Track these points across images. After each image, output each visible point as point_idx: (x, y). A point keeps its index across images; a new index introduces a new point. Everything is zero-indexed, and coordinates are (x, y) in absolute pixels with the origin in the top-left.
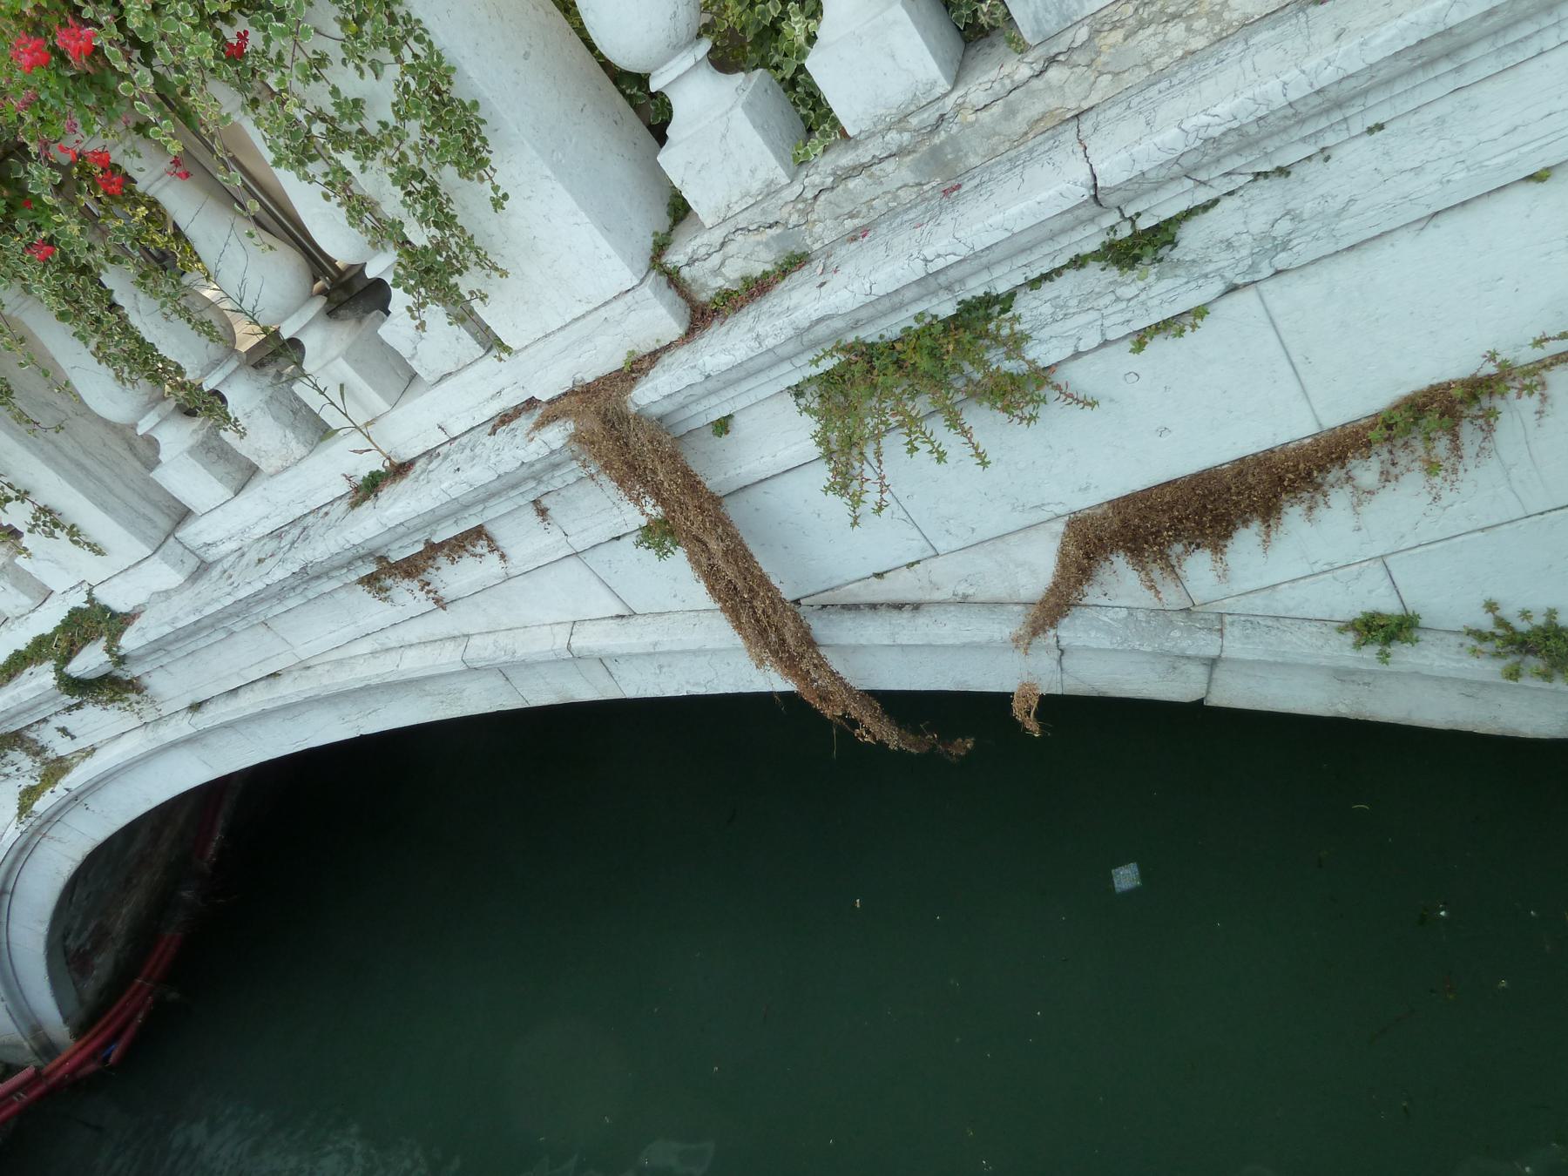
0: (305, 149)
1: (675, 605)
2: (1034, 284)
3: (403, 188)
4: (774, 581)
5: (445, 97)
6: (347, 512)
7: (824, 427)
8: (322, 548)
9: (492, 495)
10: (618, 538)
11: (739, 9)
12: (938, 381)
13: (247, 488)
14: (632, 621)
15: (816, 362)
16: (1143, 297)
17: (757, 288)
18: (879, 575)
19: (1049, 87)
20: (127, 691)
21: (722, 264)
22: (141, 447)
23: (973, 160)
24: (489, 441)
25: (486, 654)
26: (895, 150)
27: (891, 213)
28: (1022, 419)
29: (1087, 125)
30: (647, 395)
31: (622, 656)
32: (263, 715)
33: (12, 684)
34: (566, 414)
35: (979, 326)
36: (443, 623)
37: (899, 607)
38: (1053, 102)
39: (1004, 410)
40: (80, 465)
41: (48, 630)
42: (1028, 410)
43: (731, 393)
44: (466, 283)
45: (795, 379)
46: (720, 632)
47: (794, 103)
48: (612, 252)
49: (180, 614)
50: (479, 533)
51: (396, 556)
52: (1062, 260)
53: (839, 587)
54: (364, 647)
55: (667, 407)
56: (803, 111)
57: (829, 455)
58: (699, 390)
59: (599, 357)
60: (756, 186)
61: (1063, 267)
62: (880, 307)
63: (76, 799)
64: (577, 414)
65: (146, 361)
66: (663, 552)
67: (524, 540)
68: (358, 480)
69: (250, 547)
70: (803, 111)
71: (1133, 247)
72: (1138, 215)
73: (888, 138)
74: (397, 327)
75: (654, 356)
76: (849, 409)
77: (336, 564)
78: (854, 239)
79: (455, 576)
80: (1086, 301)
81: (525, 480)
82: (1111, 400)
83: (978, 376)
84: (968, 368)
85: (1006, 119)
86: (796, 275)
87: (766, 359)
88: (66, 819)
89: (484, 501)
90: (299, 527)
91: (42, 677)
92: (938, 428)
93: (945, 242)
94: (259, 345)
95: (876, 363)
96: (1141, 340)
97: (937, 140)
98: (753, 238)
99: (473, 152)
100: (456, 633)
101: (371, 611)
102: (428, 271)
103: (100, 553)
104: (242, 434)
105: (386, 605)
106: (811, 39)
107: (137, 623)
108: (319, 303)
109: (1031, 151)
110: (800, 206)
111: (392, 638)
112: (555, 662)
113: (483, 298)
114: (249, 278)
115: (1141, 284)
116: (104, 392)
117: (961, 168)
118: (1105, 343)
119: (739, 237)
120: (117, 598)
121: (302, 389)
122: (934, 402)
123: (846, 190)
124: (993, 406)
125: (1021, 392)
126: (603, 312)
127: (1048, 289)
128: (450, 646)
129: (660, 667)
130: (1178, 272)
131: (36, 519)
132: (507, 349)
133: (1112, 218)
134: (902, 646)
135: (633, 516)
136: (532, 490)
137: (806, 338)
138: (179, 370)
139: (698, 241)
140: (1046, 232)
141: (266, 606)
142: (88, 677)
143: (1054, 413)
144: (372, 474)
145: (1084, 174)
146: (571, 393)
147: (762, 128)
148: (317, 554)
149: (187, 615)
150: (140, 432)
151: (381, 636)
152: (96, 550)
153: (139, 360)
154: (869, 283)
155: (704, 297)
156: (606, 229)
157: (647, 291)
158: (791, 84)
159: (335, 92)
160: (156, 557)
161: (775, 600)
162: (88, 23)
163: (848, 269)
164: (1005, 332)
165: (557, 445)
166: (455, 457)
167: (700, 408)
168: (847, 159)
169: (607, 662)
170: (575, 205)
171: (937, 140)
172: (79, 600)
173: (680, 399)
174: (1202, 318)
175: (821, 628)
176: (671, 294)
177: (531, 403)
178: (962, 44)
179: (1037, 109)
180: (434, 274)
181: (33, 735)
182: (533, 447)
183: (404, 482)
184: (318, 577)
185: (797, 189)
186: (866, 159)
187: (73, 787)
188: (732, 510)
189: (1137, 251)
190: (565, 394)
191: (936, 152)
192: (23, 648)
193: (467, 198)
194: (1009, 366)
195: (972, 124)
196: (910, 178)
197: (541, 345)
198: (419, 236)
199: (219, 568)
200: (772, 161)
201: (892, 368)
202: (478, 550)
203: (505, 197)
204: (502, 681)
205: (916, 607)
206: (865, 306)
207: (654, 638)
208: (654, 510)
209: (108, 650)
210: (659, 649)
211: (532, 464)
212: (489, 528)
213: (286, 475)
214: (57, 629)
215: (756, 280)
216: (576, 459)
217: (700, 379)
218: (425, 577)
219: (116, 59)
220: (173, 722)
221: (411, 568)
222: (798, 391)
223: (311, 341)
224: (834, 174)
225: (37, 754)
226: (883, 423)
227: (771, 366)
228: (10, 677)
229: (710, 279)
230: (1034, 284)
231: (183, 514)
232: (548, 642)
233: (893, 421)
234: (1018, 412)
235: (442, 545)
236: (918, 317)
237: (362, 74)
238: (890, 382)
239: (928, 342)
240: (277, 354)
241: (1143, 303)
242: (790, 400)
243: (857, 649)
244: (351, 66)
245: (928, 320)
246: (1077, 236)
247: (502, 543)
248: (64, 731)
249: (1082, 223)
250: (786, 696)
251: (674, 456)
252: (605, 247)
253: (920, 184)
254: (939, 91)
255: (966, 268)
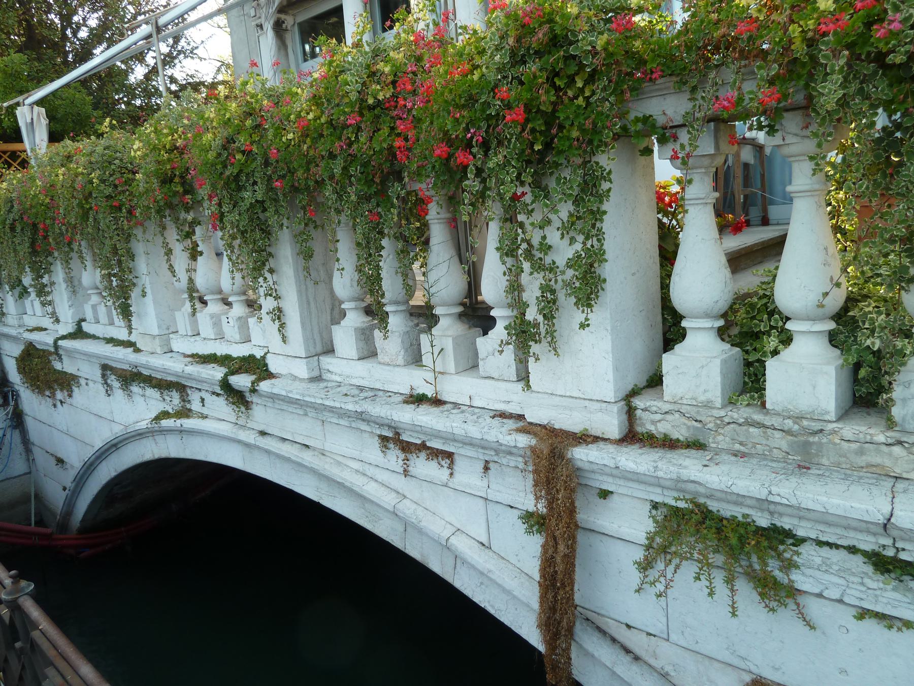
0: (513, 250)
1: (513, 560)
2: (820, 543)
3: (543, 292)
4: (576, 588)
5: (593, 269)
6: (400, 403)
7: (656, 533)
8: (378, 410)
9: (471, 444)
10: (512, 507)
11: (744, 315)
12: (734, 553)
13: (365, 360)
14: (487, 551)
15: (677, 499)
16: (878, 592)
17: (669, 444)
18: (629, 627)
19: (890, 454)
20: (243, 404)
21: (660, 421)
22: (336, 311)
23: (825, 461)
24: (489, 420)
25: (407, 512)
26: (786, 429)
27: (763, 457)
28: (767, 606)
29: (900, 486)
30: (581, 454)
31: (469, 563)
32: (288, 460)
33: (202, 366)
34: (535, 434)
35: (775, 543)
36: (400, 482)
37: (627, 651)
38: (887, 462)
39: (760, 594)
40: (308, 303)
41: (235, 355)
42: (774, 604)
43: (621, 482)
44: (535, 348)
45: (658, 499)
46: (531, 595)
47: (745, 374)
48: (612, 380)
49: (295, 391)
50: (450, 455)
51: (405, 437)
52: (845, 543)
53: (603, 616)
54: (355, 465)
55: (586, 466)
56: (747, 379)
57: (648, 547)
58: (607, 470)
59: (569, 420)
60: (702, 398)
61: (842, 546)
62: (729, 497)
63: (181, 431)
64: (541, 439)
65: (373, 284)
66: (529, 531)
67: (468, 474)
68: (415, 393)
69: (345, 385)
70: (747, 379)
71: (889, 563)
72: (903, 550)
73: (786, 421)
74: (487, 344)
75: (596, 439)
76: (677, 534)
77: (378, 421)
78: (736, 455)
79: (422, 466)
80: (842, 572)
81: (492, 449)
82: (824, 633)
83: (757, 567)
84: (754, 559)
85: (856, 454)
86: (693, 452)
87: (652, 480)
88: (168, 436)
89: (465, 444)
90: (374, 393)
91: (217, 373)
92: (719, 578)
93: (787, 491)
94: (421, 307)
95: (708, 522)
96: (863, 614)
97: (811, 439)
98: (684, 420)
99: (589, 298)
100: (401, 491)
101: (373, 452)
102: (524, 332)
103: (284, 341)
104: (386, 338)
105: (382, 455)
106: (775, 353)
107: (273, 381)
108: (460, 309)
109: (861, 478)
110: (718, 422)
111: (371, 471)
112: (437, 542)
113: (537, 359)
114: (441, 278)
115: (881, 585)
116: (344, 283)
117: (815, 460)
118: (840, 601)
119: (677, 415)
120: (273, 365)
121: (424, 339)
122: (725, 563)
123: (747, 431)
124: (755, 588)
125: (776, 592)
126: (587, 403)
127: (825, 551)
128: (394, 495)
129: (482, 583)
130: (907, 594)
131: (274, 310)
132: (528, 386)
133: (888, 542)
134: (614, 673)
135: (529, 503)
136: (490, 455)
137: (679, 485)
138: (383, 296)
139: (655, 403)
140: (847, 524)
141: (331, 415)
142: (234, 386)
143: (786, 616)
144: (423, 395)
145: (887, 510)
146: (544, 427)
147: (724, 375)
148: (374, 411)
149: (297, 393)
150: (343, 306)
151: (367, 466)
152: (284, 339)
153: (371, 282)
154: (730, 482)
155: (639, 429)
156: (616, 369)
157: (615, 408)
158: (748, 364)
159: (544, 238)
160: (305, 360)
161: (570, 598)
162: (471, 153)
163: (724, 468)
164: (787, 555)
165: (520, 445)
166: (467, 415)
167: (601, 478)
168: (758, 417)
169: (458, 561)
170: (610, 349)
171: (811, 439)
172: (259, 354)
173: (595, 467)
174: (908, 628)
175: (579, 629)
176: (625, 417)
177: (521, 417)
178: (851, 404)
179: (877, 460)
180: (523, 335)
181: (189, 392)
182: (509, 438)
183: (435, 409)
184: (364, 420)
185: (722, 413)
186: (768, 424)
187: (184, 426)
188: (581, 537)
189: (891, 567)
190: (540, 425)
191: (807, 444)
192: (219, 354)
193: (570, 315)
194: (777, 573)
195: (835, 444)
196: (785, 447)
197: (546, 396)
198: (531, 314)
199: (325, 384)
200: (718, 392)
201: (714, 530)
202: (443, 463)
203: (588, 325)
204: (402, 530)
205: (637, 658)
206: (722, 491)
207: (492, 568)
208: (542, 508)
209: (253, 383)
210: (490, 575)
211: (501, 445)
212: (456, 457)
213: (387, 368)
214: (238, 357)
215: (671, 440)
216: (524, 457)
217: (613, 465)
218: (409, 456)
219: (471, 172)
220: (248, 432)
221: (407, 448)
222: (655, 506)
223: (443, 323)
224: (746, 419)
225: (184, 401)
226: (690, 553)
227: (650, 485)
228: (204, 362)
229: (648, 423)
230: (820, 543)
231: (330, 350)
232: (437, 528)
233: (696, 555)
234: (767, 602)
235: (429, 448)
236: (745, 516)
237: (562, 237)
238: (709, 536)
239: (742, 531)
240: (425, 316)
241: (876, 596)
242: (648, 506)
243: (587, 654)
244: (560, 232)
245: (749, 520)
246: (860, 536)
247: (456, 467)
248: (203, 400)
249: (868, 532)
250: (540, 652)
251: (573, 490)
252: (610, 376)
253: (788, 453)
254: (827, 417)
255: (789, 511)
